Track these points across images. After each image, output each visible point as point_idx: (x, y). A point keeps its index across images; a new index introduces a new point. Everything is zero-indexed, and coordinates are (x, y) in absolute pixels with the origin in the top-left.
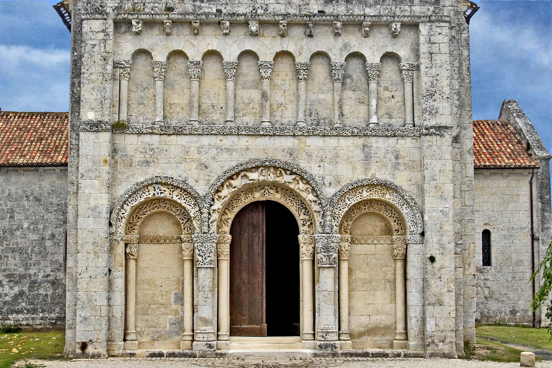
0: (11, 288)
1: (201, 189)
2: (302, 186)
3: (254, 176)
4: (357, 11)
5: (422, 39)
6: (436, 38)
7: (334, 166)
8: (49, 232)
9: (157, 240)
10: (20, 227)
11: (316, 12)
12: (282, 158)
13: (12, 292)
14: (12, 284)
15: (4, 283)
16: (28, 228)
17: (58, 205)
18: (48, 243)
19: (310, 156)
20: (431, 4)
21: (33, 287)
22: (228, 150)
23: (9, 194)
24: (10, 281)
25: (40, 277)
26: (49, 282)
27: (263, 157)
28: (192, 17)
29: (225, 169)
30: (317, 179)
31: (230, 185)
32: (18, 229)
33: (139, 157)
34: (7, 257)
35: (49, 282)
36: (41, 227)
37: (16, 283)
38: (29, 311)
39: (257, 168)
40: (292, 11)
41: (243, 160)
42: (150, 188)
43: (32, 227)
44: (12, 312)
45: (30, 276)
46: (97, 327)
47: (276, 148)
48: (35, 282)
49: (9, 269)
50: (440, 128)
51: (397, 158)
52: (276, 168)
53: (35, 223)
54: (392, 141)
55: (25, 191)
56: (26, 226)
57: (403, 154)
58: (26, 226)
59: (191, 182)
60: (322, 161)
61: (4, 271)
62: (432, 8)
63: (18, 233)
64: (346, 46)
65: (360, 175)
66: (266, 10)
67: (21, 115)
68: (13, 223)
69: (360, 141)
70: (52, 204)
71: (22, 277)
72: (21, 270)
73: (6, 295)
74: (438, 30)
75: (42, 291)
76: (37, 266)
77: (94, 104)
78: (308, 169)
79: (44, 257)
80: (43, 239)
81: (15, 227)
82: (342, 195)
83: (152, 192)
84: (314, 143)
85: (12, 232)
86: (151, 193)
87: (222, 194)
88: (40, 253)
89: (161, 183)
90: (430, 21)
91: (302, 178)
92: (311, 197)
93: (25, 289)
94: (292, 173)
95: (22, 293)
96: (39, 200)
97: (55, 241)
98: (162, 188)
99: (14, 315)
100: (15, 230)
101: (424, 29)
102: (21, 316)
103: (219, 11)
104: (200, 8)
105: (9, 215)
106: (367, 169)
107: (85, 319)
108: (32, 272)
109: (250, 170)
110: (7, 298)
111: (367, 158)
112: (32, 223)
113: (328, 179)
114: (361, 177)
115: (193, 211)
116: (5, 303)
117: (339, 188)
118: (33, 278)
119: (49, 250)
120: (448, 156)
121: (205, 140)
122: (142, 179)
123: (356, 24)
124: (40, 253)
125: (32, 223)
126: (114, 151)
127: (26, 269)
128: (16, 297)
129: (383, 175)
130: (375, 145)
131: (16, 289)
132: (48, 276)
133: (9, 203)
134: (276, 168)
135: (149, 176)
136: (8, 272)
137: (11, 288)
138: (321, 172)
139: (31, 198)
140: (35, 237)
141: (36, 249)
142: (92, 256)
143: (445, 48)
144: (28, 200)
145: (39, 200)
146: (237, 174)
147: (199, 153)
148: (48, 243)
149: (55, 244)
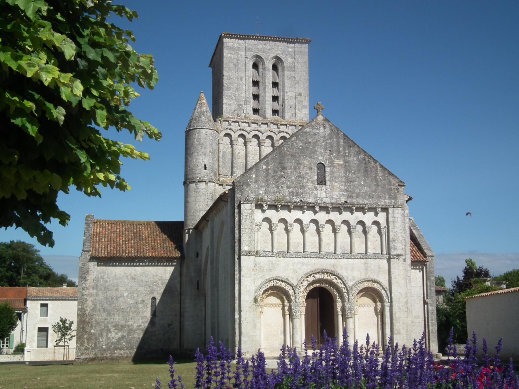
0: (116, 334)
1: (294, 282)
2: (339, 281)
3: (318, 276)
4: (361, 202)
5: (390, 216)
6: (395, 215)
7: (352, 273)
8: (141, 299)
9: (273, 306)
10: (122, 296)
11: (343, 202)
12: (329, 268)
13: (117, 336)
14: (117, 331)
15: (112, 330)
16: (127, 296)
17: (147, 282)
18: (140, 306)
19: (342, 268)
20: (393, 199)
21: (130, 333)
22: (306, 264)
23: (115, 275)
24: (116, 329)
25: (135, 327)
26: (141, 330)
27: (321, 268)
28: (290, 204)
29: (305, 273)
30: (345, 278)
31: (307, 280)
32: (121, 297)
33: (266, 267)
34: (114, 314)
35: (141, 330)
36: (135, 295)
37: (120, 331)
38: (127, 348)
39: (319, 273)
40: (333, 201)
41: (313, 269)
42: (272, 281)
43: (130, 296)
44: (116, 349)
45: (128, 326)
46: (251, 346)
47: (327, 264)
48: (131, 330)
49: (115, 322)
50: (398, 255)
51: (379, 269)
52: (327, 273)
53: (132, 293)
54: (377, 260)
55: (125, 273)
56: (126, 294)
57: (382, 267)
58: (126, 294)
59: (290, 279)
60: (347, 269)
61: (112, 323)
62: (393, 201)
63: (121, 299)
64: (357, 217)
65: (363, 277)
66: (322, 200)
67: (110, 223)
68: (118, 293)
69: (363, 261)
70: (143, 281)
71: (123, 327)
72: (123, 322)
73: (113, 338)
74: (397, 211)
75: (136, 336)
76: (133, 320)
77: (248, 243)
78: (341, 274)
79: (138, 314)
80: (137, 303)
81: (119, 295)
82: (355, 285)
83: (273, 283)
84: (344, 261)
85: (117, 299)
86: (283, 285)
87: (304, 284)
88: (135, 312)
89: (277, 280)
90: (394, 207)
91: (339, 278)
92: (343, 286)
93: (125, 334)
94: (334, 275)
95: (123, 337)
96: (134, 279)
97: (144, 304)
98: (278, 282)
99: (119, 351)
100: (119, 297)
101: (391, 210)
102: (122, 352)
103: (301, 200)
104: (293, 199)
105: (115, 288)
106: (367, 273)
107: (246, 342)
108: (130, 323)
109: (316, 273)
110: (114, 340)
111: (366, 269)
112: (130, 293)
113: (350, 278)
114: (364, 277)
115: (291, 292)
116: (112, 343)
117: (355, 282)
118: (130, 327)
119: (140, 310)
120: (401, 268)
121: (296, 260)
122: (268, 278)
123: (361, 209)
124: (135, 312)
125: (130, 293)
126: (255, 265)
127: (126, 322)
128: (119, 339)
129: (374, 277)
130: (369, 263)
131: (120, 334)
132: (140, 326)
133: (115, 281)
134: (327, 273)
135: (271, 276)
136: (114, 324)
137: (116, 334)
138: (347, 275)
139: (129, 277)
140: (132, 302)
141: (132, 309)
142: (248, 313)
143: (399, 220)
144: (127, 278)
145: (134, 279)
146: (310, 275)
147: (293, 265)
148: (140, 306)
149: (144, 306)
